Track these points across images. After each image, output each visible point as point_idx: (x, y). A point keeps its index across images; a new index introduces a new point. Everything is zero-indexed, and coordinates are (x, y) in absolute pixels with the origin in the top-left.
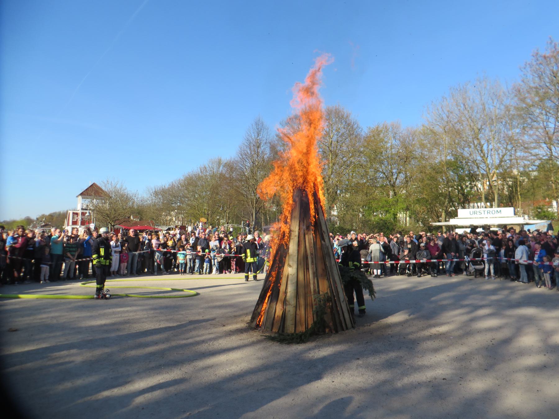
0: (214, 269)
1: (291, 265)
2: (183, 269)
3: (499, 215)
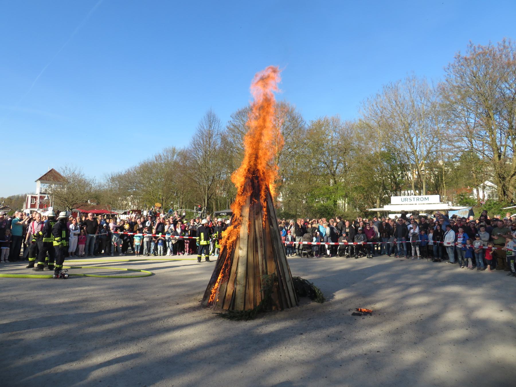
0: (169, 251)
1: (242, 248)
2: (138, 251)
3: (427, 202)
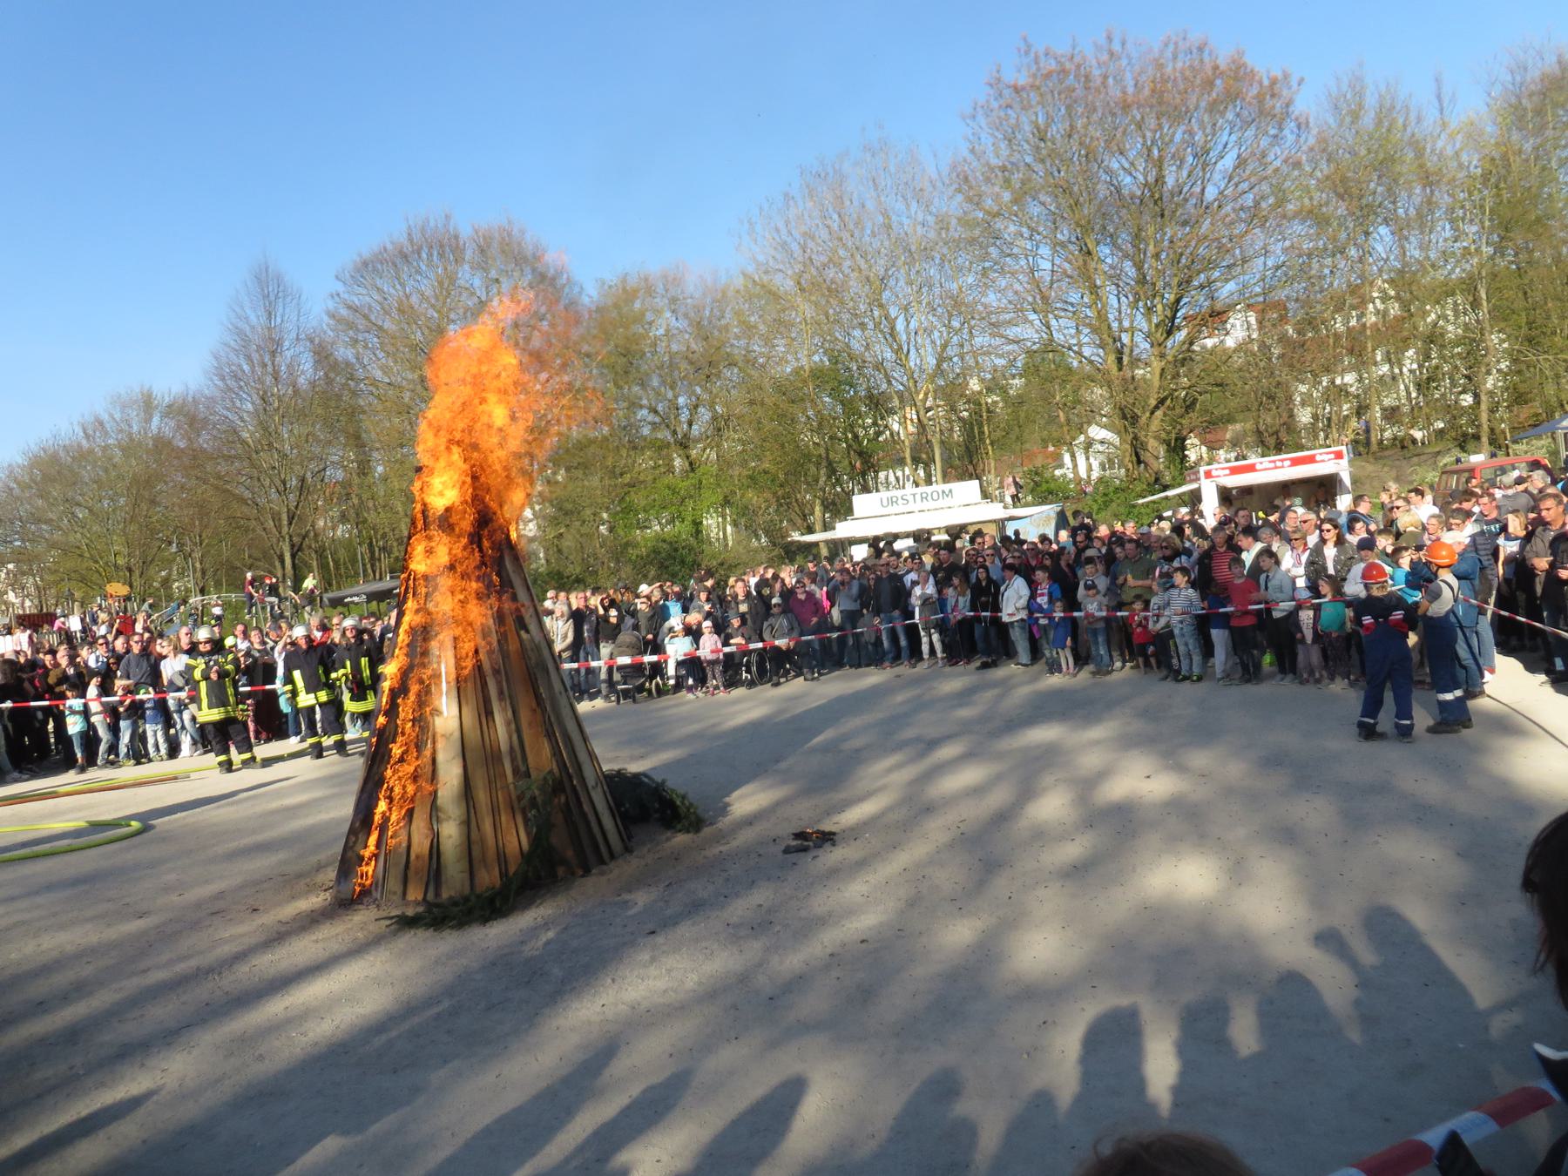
3: (947, 501)
